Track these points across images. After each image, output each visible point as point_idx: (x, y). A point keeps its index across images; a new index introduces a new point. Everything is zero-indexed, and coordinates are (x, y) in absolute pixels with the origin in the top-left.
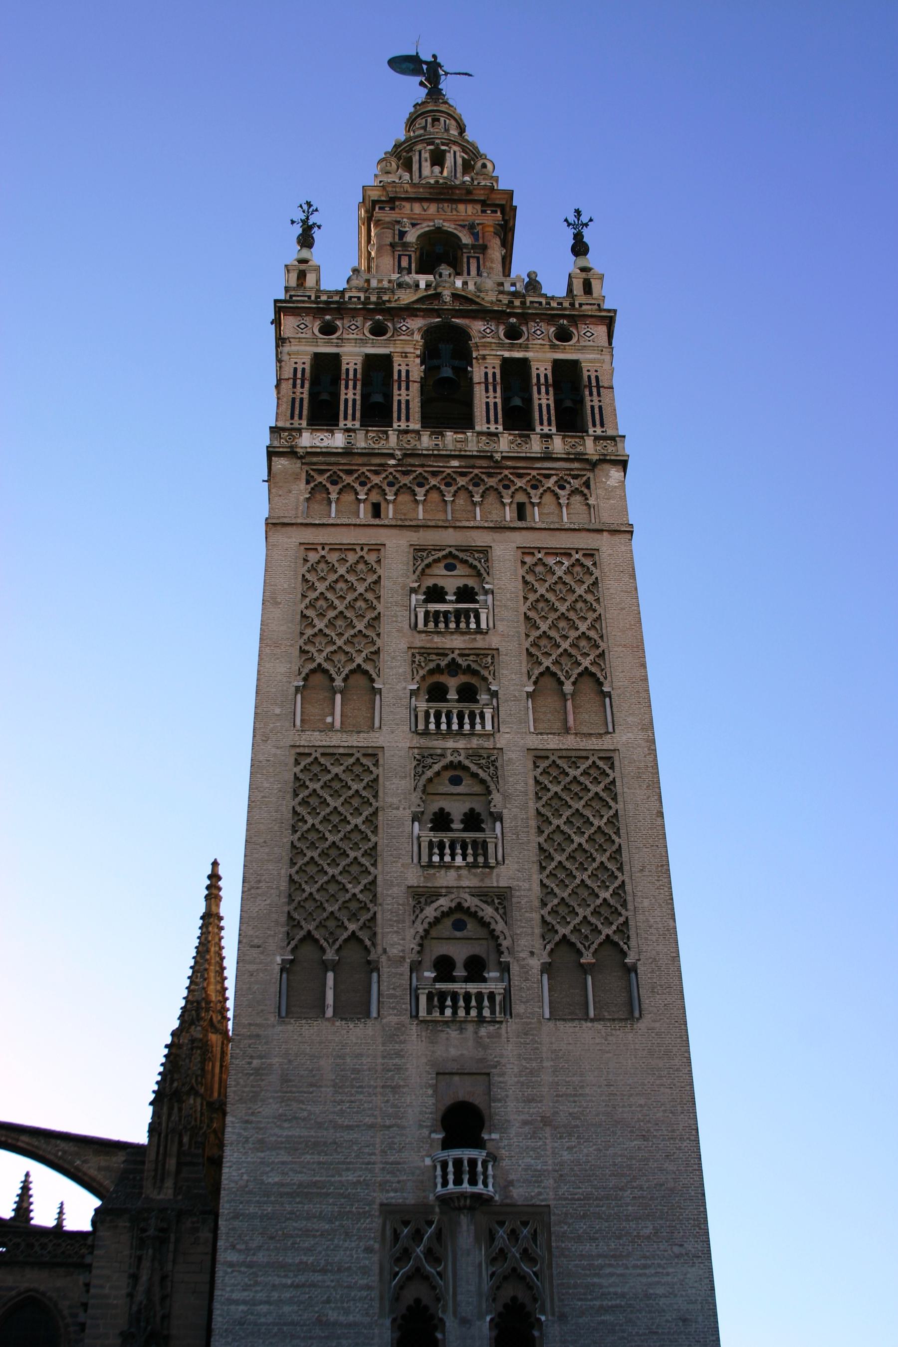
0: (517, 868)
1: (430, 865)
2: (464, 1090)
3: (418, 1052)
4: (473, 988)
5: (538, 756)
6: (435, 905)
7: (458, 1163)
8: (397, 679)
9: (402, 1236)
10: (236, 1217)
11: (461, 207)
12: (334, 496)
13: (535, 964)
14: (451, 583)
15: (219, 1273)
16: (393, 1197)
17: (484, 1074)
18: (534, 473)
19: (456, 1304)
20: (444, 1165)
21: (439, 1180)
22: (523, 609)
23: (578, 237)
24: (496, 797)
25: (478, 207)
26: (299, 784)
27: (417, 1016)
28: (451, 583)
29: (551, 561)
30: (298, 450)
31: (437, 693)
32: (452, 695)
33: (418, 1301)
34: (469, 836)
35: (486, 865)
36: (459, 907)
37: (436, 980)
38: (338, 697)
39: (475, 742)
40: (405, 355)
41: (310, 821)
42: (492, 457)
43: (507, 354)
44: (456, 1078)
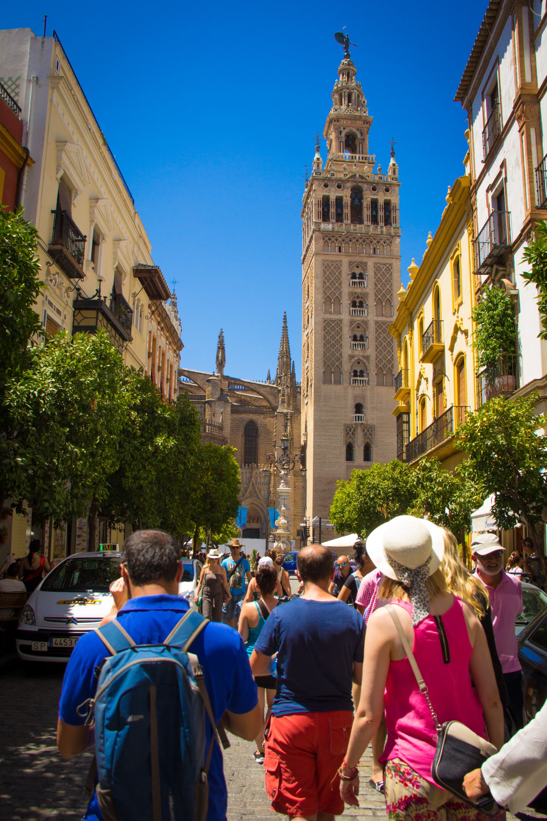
0: (371, 351)
2: (359, 401)
3: (350, 392)
5: (376, 322)
8: (346, 301)
16: (346, 422)
17: (364, 397)
23: (392, 149)
24: (367, 333)
26: (325, 328)
28: (358, 271)
29: (381, 267)
32: (358, 304)
34: (361, 343)
39: (363, 318)
40: (346, 196)
43: (372, 197)
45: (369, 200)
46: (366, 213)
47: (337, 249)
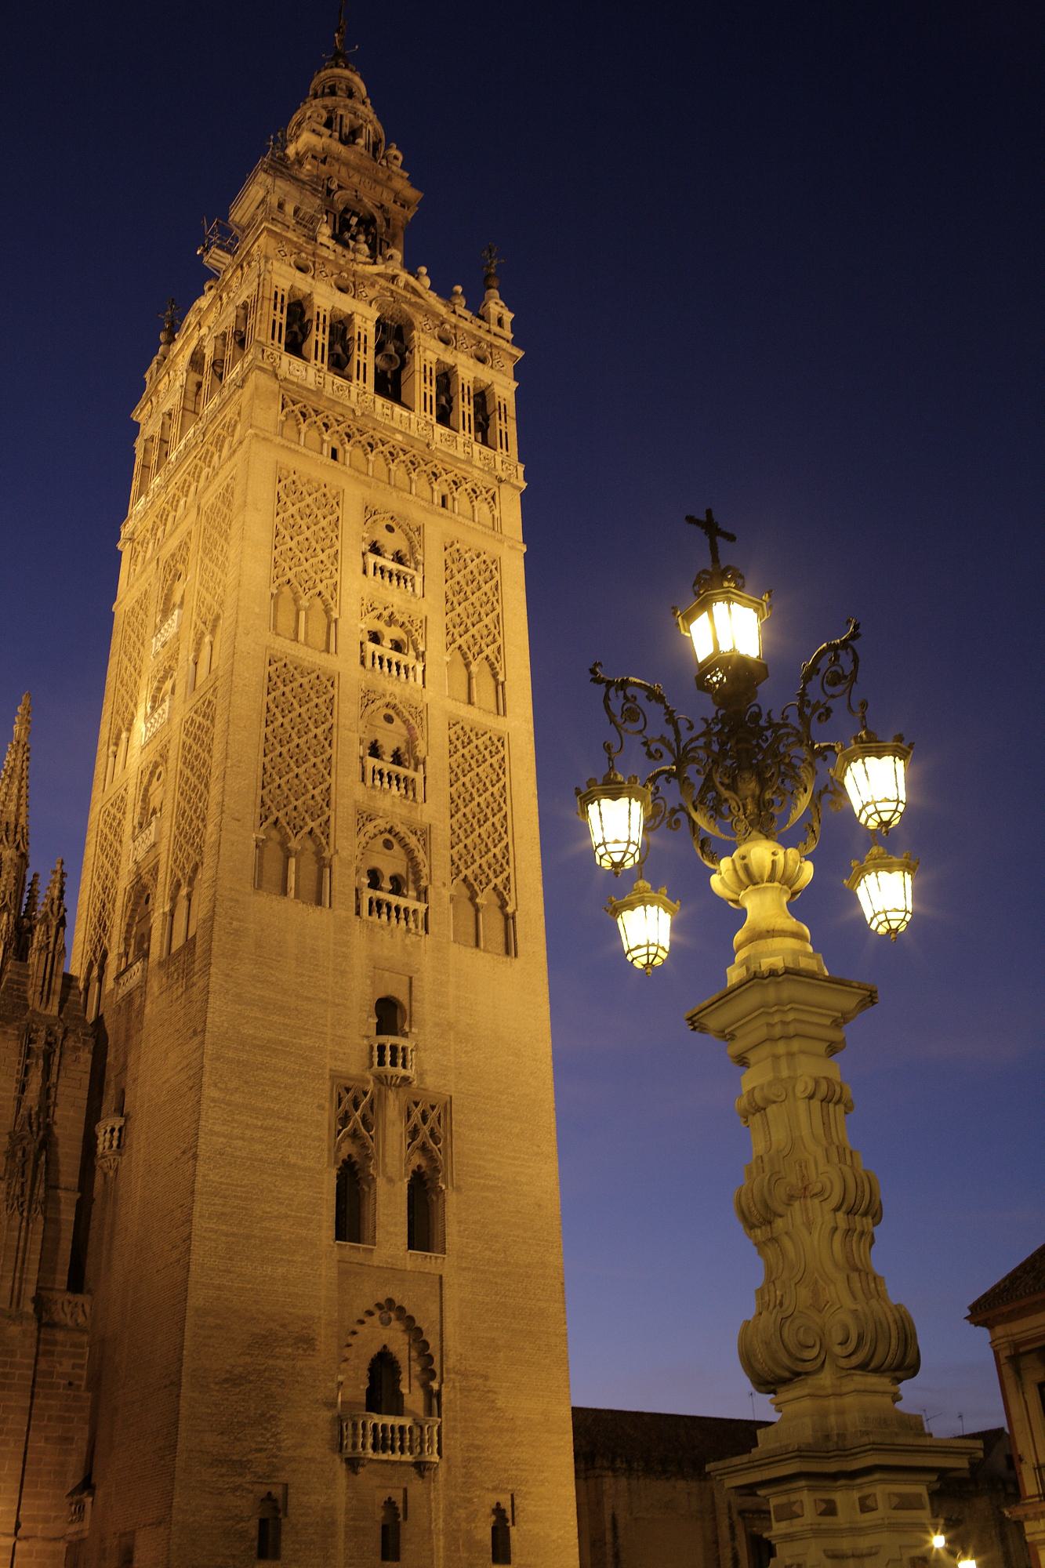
0: (434, 811)
1: (374, 787)
4: (394, 900)
6: (374, 823)
7: (394, 1048)
9: (345, 1100)
10: (218, 1059)
11: (379, 189)
12: (304, 427)
13: (446, 893)
14: (393, 542)
15: (204, 1107)
18: (457, 471)
19: (385, 1165)
20: (382, 1048)
21: (376, 1060)
22: (446, 587)
25: (392, 197)
27: (358, 913)
28: (393, 542)
30: (279, 372)
31: (375, 638)
32: (387, 643)
33: (350, 1156)
35: (414, 800)
36: (390, 831)
37: (370, 886)
38: (302, 614)
41: (281, 720)
42: (428, 445)
44: (387, 974)
45: (431, 357)
46: (421, 388)
47: (327, 450)
